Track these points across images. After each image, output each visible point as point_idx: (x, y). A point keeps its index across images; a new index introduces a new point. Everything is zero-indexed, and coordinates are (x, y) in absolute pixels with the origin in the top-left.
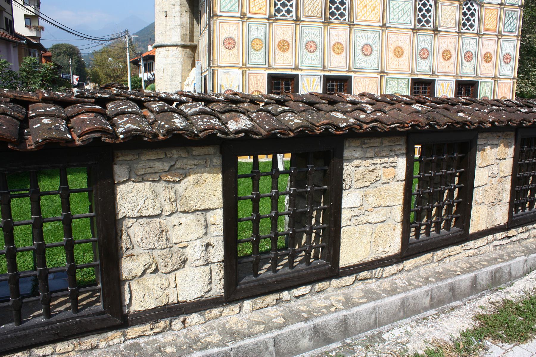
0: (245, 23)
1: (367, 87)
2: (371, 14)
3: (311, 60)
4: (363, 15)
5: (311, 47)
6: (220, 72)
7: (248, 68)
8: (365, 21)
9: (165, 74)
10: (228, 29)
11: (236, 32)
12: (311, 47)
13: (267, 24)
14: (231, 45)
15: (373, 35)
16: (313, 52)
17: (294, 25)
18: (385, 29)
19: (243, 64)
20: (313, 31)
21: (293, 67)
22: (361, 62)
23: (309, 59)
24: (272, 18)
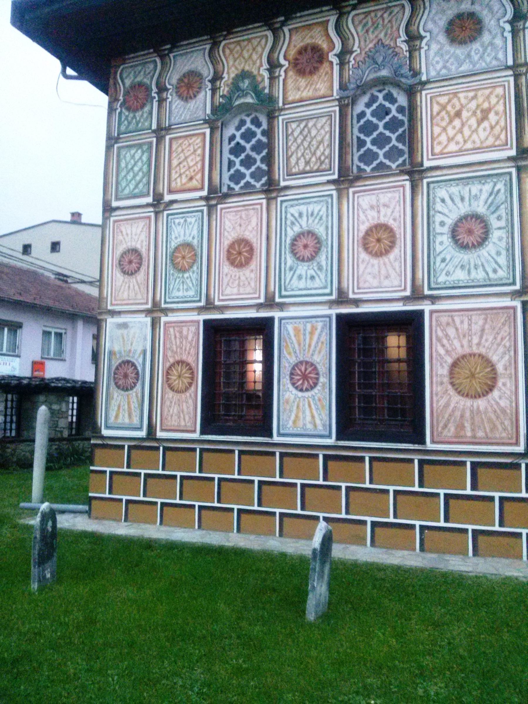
1: (475, 340)
4: (450, 140)
5: (305, 246)
6: (111, 322)
7: (165, 311)
10: (129, 232)
11: (143, 236)
13: (205, 209)
14: (134, 266)
16: (312, 258)
17: (264, 202)
19: (155, 304)
20: (311, 208)
21: (262, 300)
22: (450, 268)
23: (300, 277)
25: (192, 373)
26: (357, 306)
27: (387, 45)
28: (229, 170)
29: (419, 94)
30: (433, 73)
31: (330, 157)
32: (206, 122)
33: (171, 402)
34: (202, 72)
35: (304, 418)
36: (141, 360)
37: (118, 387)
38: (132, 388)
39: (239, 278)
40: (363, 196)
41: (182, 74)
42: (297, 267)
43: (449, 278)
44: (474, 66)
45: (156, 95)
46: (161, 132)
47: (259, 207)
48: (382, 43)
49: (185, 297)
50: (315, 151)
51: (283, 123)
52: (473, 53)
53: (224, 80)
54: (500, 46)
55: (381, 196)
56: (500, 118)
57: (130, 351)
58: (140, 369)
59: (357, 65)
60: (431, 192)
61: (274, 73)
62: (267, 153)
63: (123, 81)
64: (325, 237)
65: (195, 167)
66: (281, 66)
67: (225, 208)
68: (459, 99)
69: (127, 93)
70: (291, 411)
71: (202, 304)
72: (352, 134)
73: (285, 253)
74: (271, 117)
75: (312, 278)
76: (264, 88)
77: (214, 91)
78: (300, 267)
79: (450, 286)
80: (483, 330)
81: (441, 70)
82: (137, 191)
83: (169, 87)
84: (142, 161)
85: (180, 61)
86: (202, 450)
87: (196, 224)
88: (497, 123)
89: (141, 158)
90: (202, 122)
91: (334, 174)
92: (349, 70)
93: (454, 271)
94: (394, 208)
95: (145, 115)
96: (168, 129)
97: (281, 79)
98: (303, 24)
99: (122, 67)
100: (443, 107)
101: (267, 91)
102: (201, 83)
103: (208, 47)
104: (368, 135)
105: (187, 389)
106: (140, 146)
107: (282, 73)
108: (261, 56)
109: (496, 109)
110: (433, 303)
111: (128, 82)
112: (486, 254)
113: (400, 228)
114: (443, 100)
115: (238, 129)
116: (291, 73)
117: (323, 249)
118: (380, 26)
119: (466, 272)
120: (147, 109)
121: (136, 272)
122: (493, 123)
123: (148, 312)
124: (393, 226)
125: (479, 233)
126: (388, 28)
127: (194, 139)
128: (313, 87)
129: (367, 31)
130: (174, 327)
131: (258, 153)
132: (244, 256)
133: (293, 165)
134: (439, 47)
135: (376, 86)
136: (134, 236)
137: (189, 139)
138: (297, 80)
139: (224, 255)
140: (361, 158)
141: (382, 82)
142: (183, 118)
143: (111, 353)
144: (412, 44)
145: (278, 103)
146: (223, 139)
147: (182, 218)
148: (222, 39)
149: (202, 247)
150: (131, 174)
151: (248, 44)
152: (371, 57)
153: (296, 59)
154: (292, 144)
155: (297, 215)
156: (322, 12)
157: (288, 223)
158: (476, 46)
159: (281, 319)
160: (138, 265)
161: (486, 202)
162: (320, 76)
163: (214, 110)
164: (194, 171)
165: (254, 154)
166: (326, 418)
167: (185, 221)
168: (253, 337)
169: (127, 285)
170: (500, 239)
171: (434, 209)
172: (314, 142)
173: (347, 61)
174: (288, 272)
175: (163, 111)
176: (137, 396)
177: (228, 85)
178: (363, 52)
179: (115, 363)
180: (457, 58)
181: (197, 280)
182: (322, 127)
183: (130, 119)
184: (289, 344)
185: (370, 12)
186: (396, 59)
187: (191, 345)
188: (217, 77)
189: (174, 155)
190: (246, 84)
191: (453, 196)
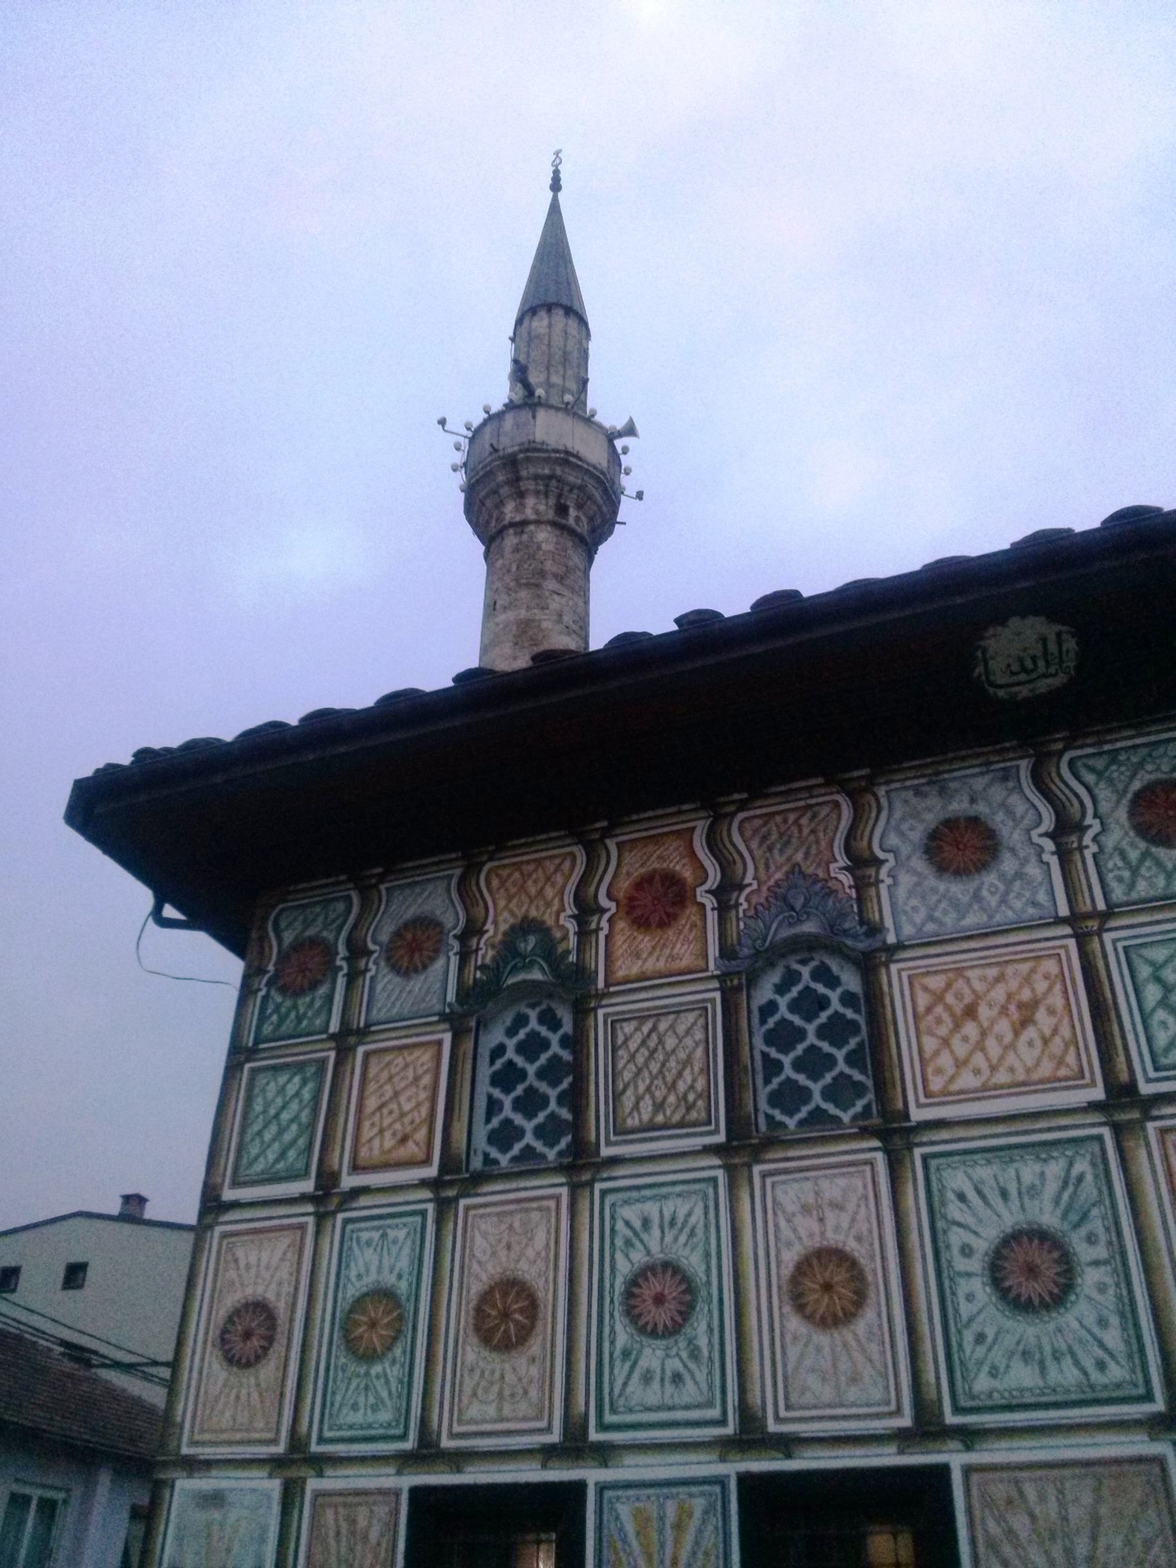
0: (329, 1224)
2: (1012, 1046)
3: (661, 1383)
4: (960, 1064)
5: (659, 1300)
7: (320, 1463)
10: (253, 1259)
12: (661, 1300)
15: (1055, 1169)
16: (673, 1330)
17: (564, 1191)
18: (1136, 1115)
19: (297, 1443)
21: (555, 1437)
22: (997, 1356)
23: (647, 1378)
26: (789, 1456)
27: (810, 876)
28: (488, 1120)
29: (883, 971)
30: (908, 930)
31: (707, 1095)
32: (444, 1017)
34: (442, 919)
39: (502, 1377)
40: (784, 1182)
41: (401, 921)
42: (640, 1352)
43: (997, 1384)
44: (991, 917)
45: (344, 965)
46: (346, 1040)
47: (552, 1204)
48: (801, 872)
49: (370, 1426)
50: (674, 1083)
51: (605, 1022)
52: (985, 893)
53: (486, 936)
54: (1040, 879)
55: (824, 1184)
56: (1060, 1021)
59: (752, 913)
60: (933, 1178)
61: (588, 923)
62: (571, 1084)
64: (704, 1279)
65: (416, 1114)
66: (603, 911)
67: (476, 1207)
68: (968, 980)
69: (283, 958)
71: (409, 1445)
72: (752, 1049)
73: (612, 1315)
74: (582, 1011)
75: (677, 1378)
76: (568, 952)
77: (465, 956)
78: (647, 1351)
79: (1003, 1402)
80: (1096, 1521)
81: (923, 924)
82: (281, 1166)
83: (372, 947)
87: (409, 1243)
88: (1055, 1031)
89: (297, 1094)
90: (435, 1018)
91: (716, 1131)
92: (738, 919)
93: (1008, 1366)
94: (856, 1213)
95: (317, 1004)
96: (363, 1033)
98: (644, 834)
99: (281, 906)
101: (572, 958)
102: (440, 941)
103: (458, 872)
104: (785, 1050)
106: (300, 1067)
107: (604, 924)
109: (1050, 1000)
110: (969, 1448)
111: (288, 937)
112: (1075, 1325)
113: (872, 1258)
114: (936, 983)
115: (511, 1032)
116: (621, 925)
118: (794, 840)
119: (1037, 1371)
120: (322, 990)
121: (258, 1358)
122: (1047, 1032)
123: (276, 1464)
124: (856, 1254)
125: (1051, 1273)
126: (809, 848)
128: (667, 951)
131: (554, 1084)
132: (516, 1322)
133: (627, 1110)
134: (915, 879)
135: (793, 951)
136: (263, 1272)
137: (406, 1053)
138: (635, 938)
140: (775, 1099)
141: (805, 946)
142: (395, 1011)
144: (859, 873)
145: (596, 984)
146: (480, 1050)
147: (378, 1228)
148: (485, 858)
150: (273, 1128)
151: (535, 870)
152: (781, 897)
153: (631, 899)
154: (624, 1067)
155: (637, 1224)
156: (680, 812)
157: (619, 1242)
158: (990, 878)
159: (602, 1488)
160: (264, 1343)
161: (1057, 1201)
162: (681, 932)
163: (463, 993)
164: (412, 1122)
165: (543, 1087)
167: (384, 1236)
168: (531, 1537)
170: (1102, 1288)
171: (944, 1217)
172: (672, 1063)
173: (732, 902)
174: (618, 1363)
177: (493, 947)
178: (764, 888)
180: (955, 904)
181: (401, 1382)
182: (688, 1032)
183: (283, 1010)
184: (624, 1558)
186: (831, 902)
187: (376, 1556)
188: (473, 929)
189: (372, 1086)
191: (980, 1187)
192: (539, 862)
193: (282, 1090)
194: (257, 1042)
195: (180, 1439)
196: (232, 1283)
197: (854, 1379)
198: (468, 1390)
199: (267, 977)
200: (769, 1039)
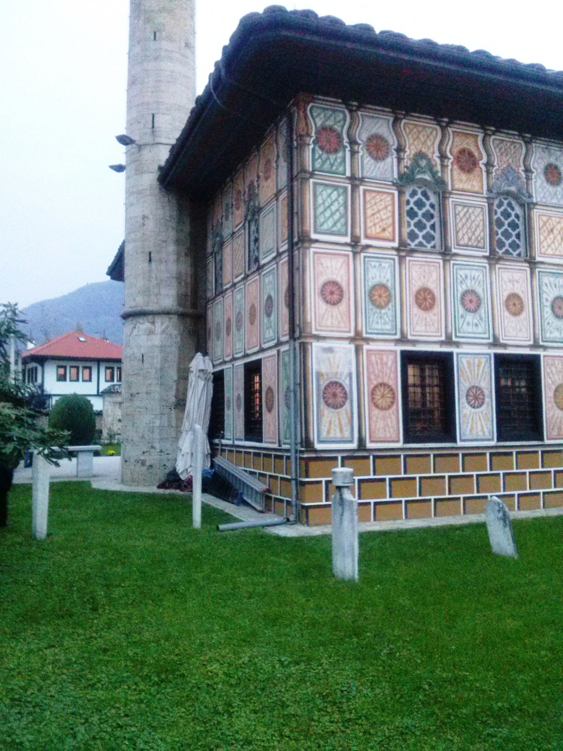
0: (358, 256)
4: (549, 246)
5: (471, 301)
6: (315, 347)
7: (367, 340)
8: (553, 256)
9: (146, 365)
10: (329, 265)
11: (343, 271)
12: (471, 301)
13: (396, 258)
14: (335, 297)
16: (475, 311)
17: (441, 261)
21: (443, 338)
23: (468, 324)
24: (403, 250)
25: (394, 394)
26: (506, 349)
30: (539, 199)
31: (483, 238)
32: (394, 184)
33: (377, 418)
35: (477, 427)
36: (347, 382)
37: (328, 405)
38: (341, 406)
45: (347, 145)
46: (355, 181)
53: (406, 154)
55: (514, 274)
57: (337, 373)
58: (347, 389)
63: (314, 119)
66: (449, 159)
69: (318, 132)
70: (468, 423)
71: (398, 336)
76: (437, 172)
77: (400, 160)
78: (468, 317)
82: (335, 229)
83: (359, 142)
84: (339, 203)
85: (368, 121)
86: (406, 457)
90: (390, 183)
91: (486, 252)
95: (339, 161)
96: (362, 180)
97: (450, 168)
100: (545, 224)
101: (440, 174)
103: (392, 119)
105: (390, 407)
107: (450, 164)
108: (433, 144)
111: (319, 123)
114: (545, 219)
116: (455, 167)
117: (482, 306)
120: (340, 154)
123: (352, 340)
127: (385, 196)
129: (502, 154)
130: (375, 354)
139: (412, 299)
141: (508, 194)
143: (319, 375)
145: (448, 187)
149: (395, 290)
151: (422, 131)
155: (464, 276)
159: (458, 354)
160: (338, 297)
164: (386, 224)
166: (490, 427)
167: (380, 265)
169: (330, 314)
172: (473, 225)
175: (356, 161)
176: (346, 413)
179: (323, 384)
182: (478, 215)
185: (503, 140)
189: (368, 205)
190: (423, 163)
192: (425, 127)
193: (329, 196)
194: (314, 170)
195: (311, 327)
196: (322, 273)
197: (520, 330)
198: (415, 323)
199: (312, 139)
200: (518, 227)
